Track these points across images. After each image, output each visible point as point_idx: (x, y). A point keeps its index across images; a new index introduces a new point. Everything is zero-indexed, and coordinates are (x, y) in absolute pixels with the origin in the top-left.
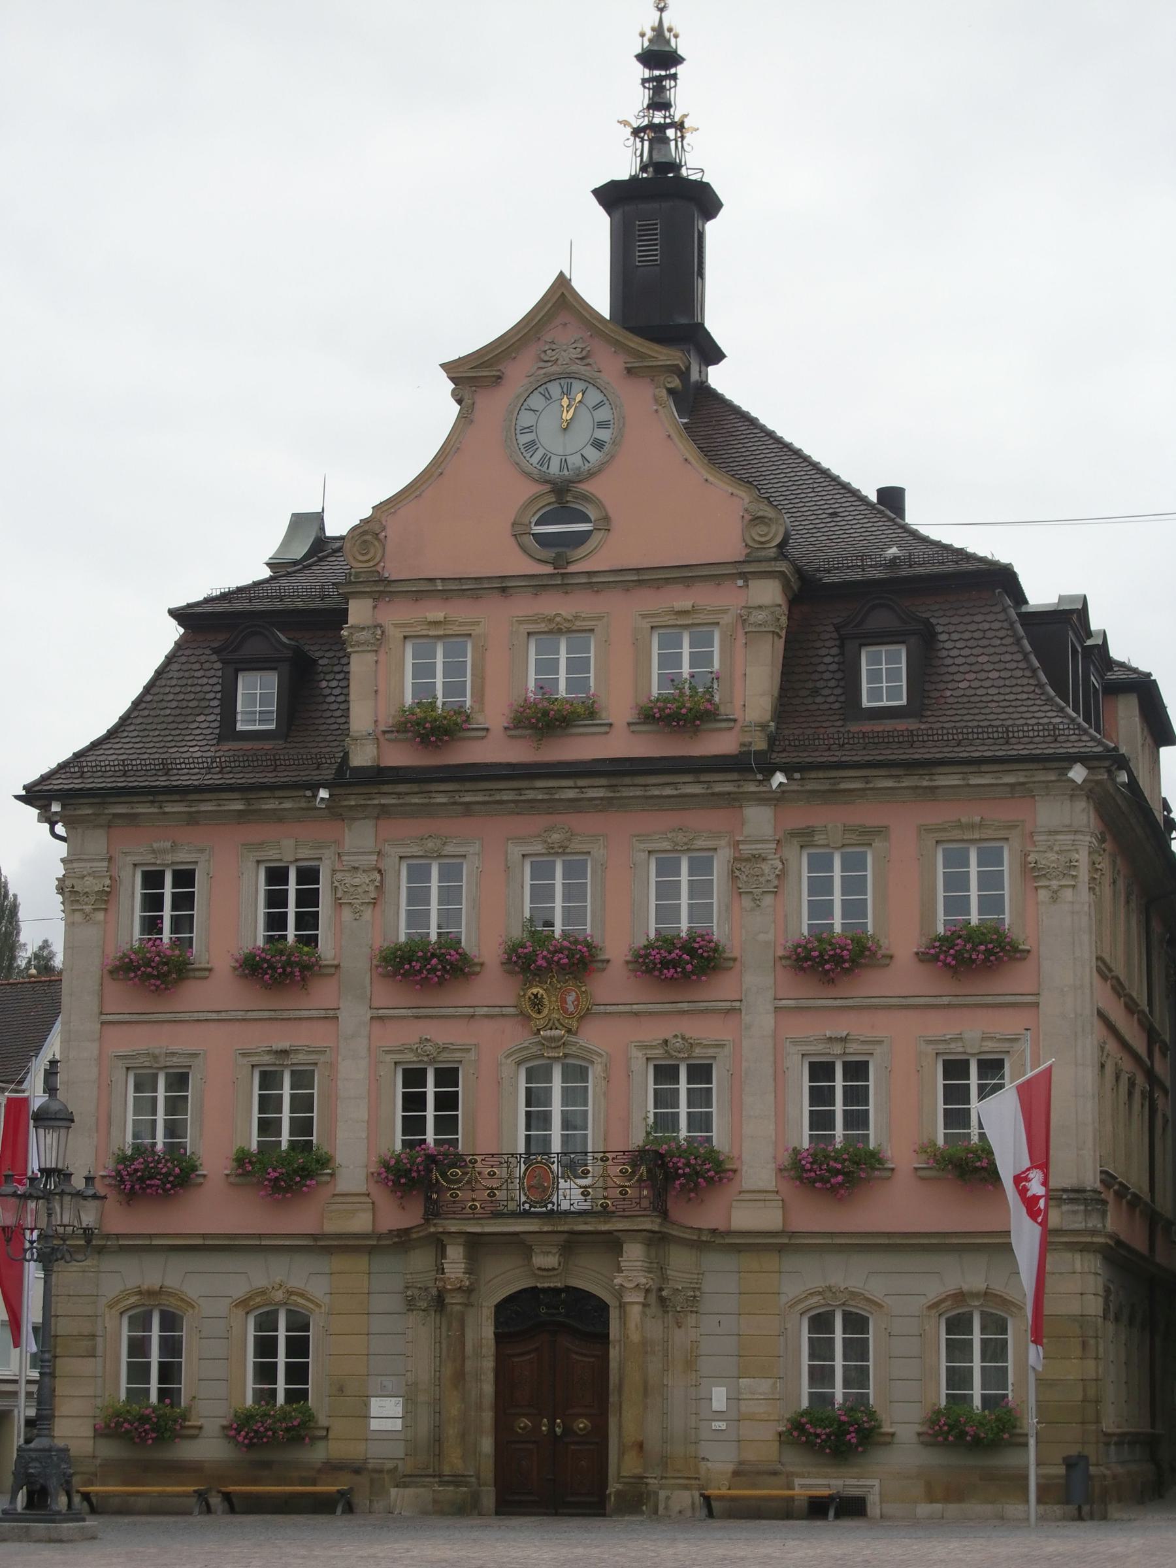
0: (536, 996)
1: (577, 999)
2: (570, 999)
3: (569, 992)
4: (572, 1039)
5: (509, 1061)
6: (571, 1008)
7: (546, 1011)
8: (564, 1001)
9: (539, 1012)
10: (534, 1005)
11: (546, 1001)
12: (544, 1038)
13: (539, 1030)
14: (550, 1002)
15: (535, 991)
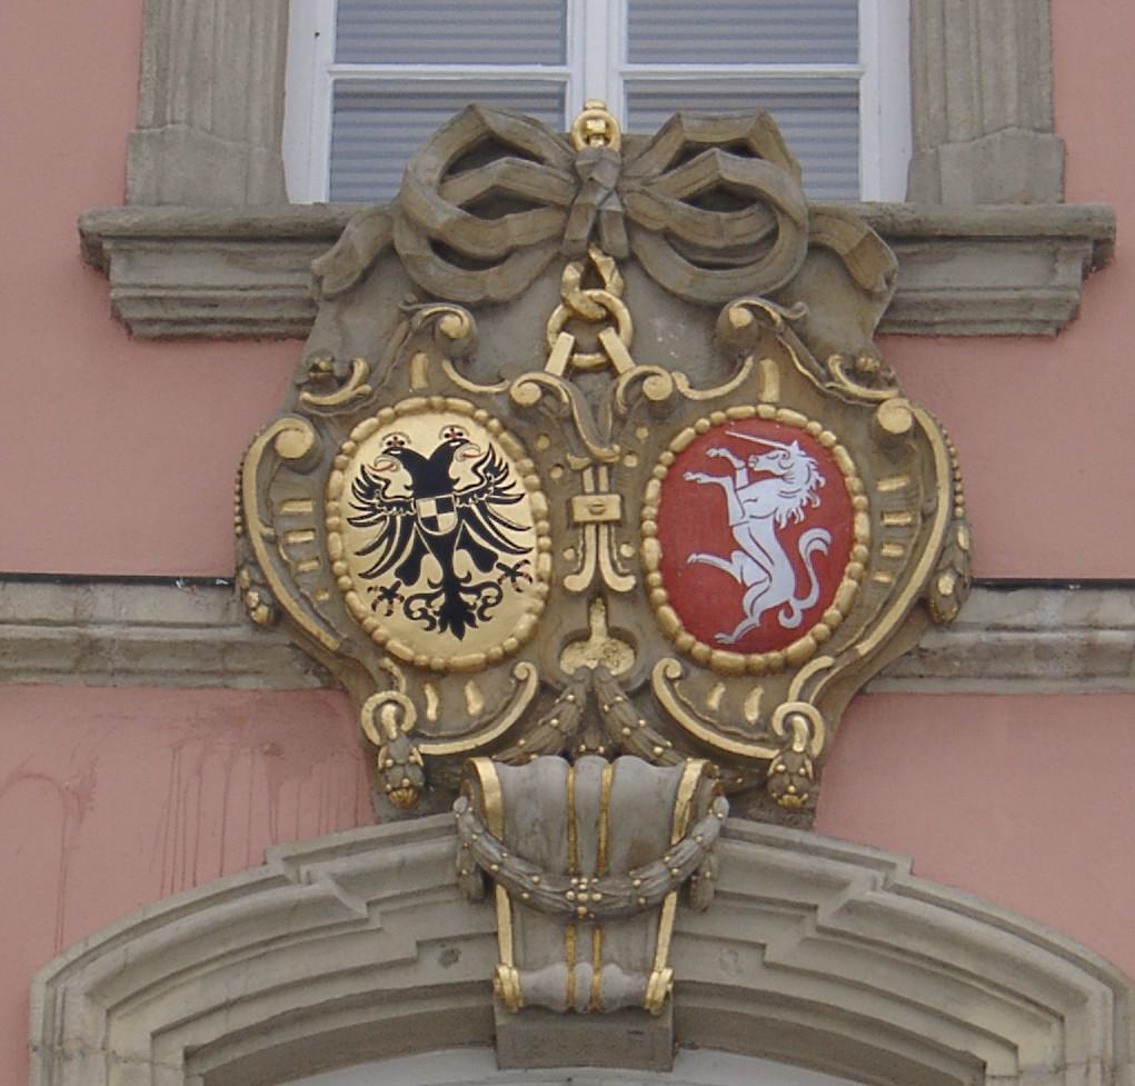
0: (431, 474)
1: (831, 507)
2: (765, 501)
3: (745, 443)
4: (765, 848)
5: (131, 1034)
6: (764, 578)
7: (514, 616)
8: (698, 520)
9: (456, 617)
10: (410, 546)
11: (521, 515)
12: (504, 822)
13: (443, 783)
14: (562, 528)
15: (424, 436)
